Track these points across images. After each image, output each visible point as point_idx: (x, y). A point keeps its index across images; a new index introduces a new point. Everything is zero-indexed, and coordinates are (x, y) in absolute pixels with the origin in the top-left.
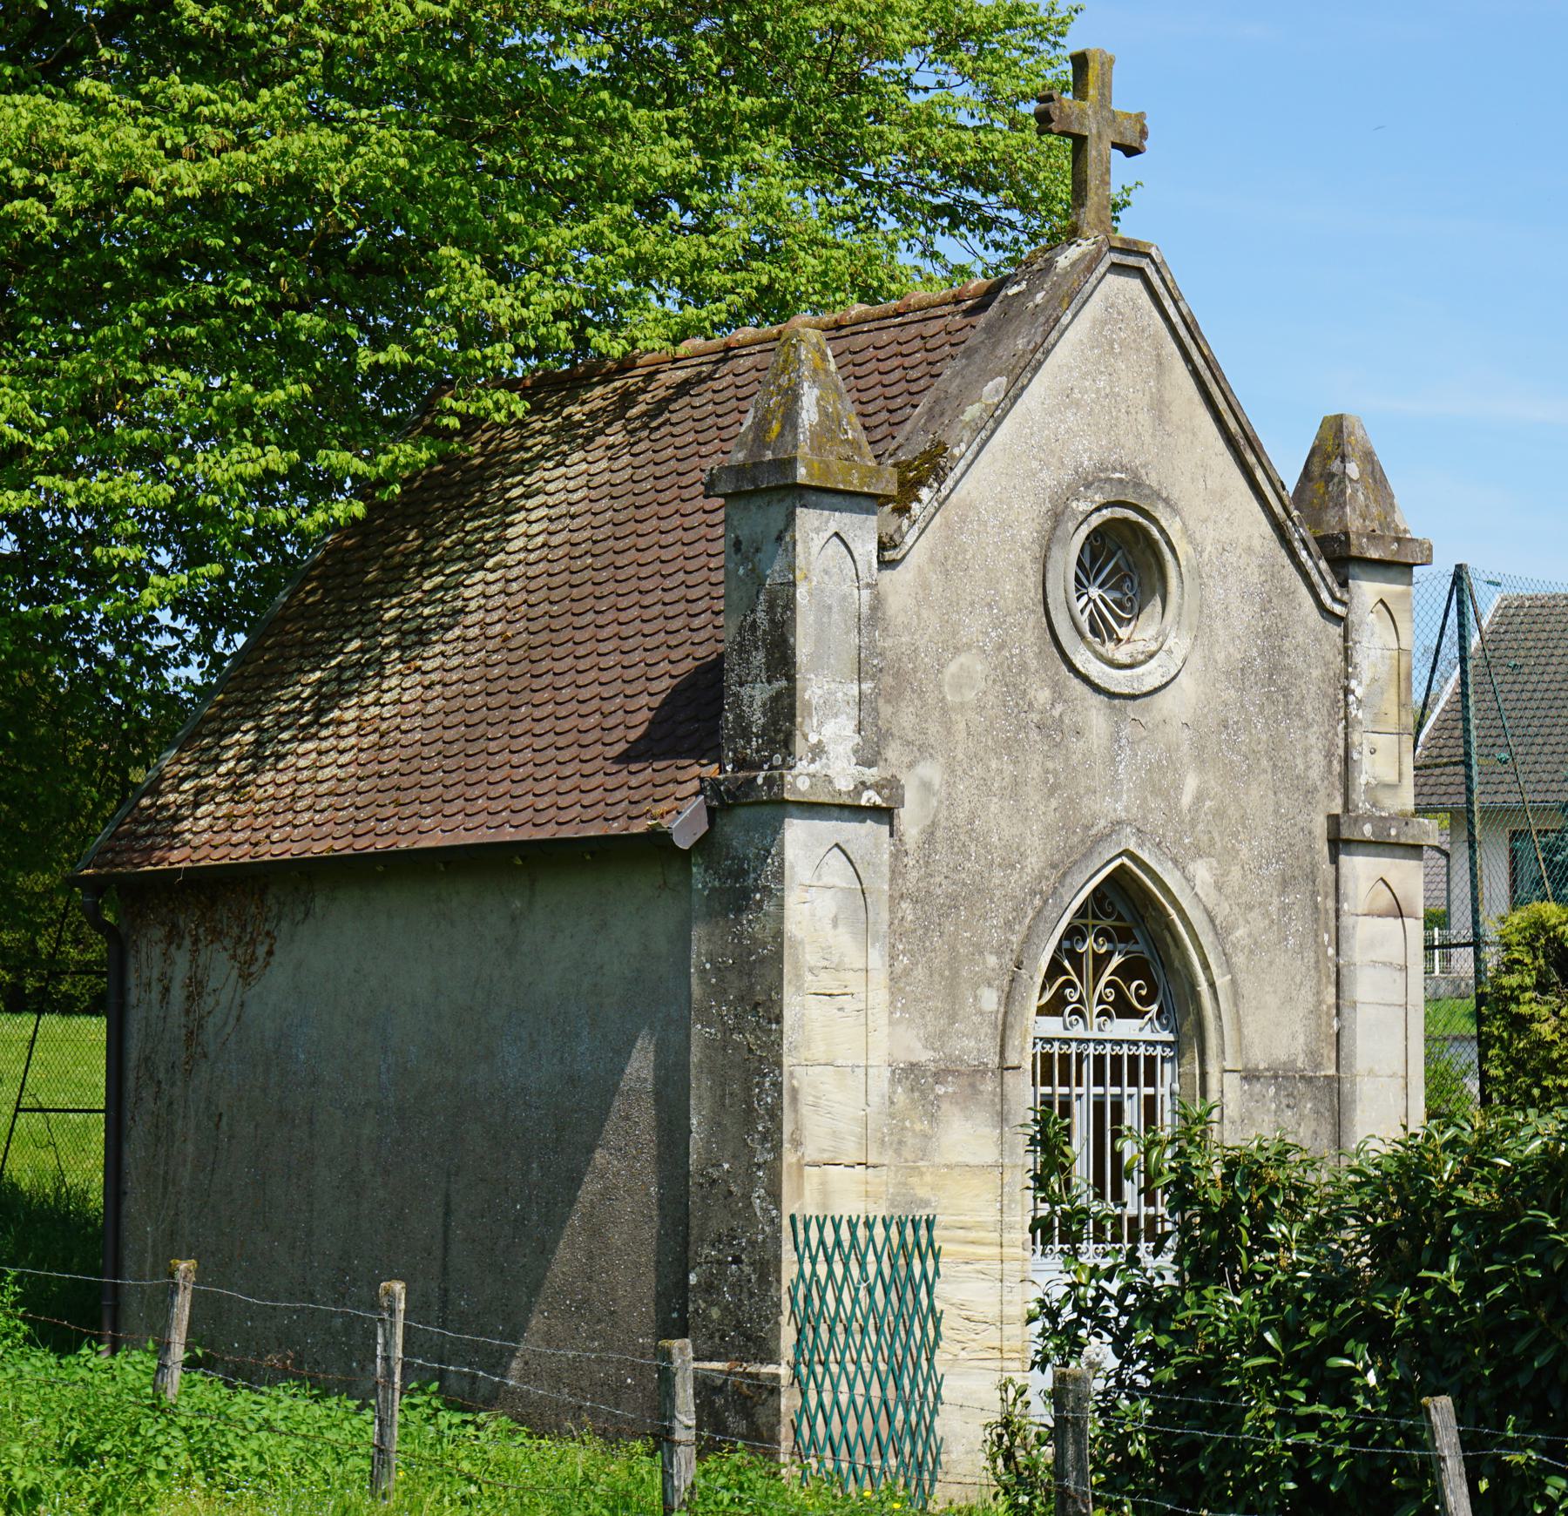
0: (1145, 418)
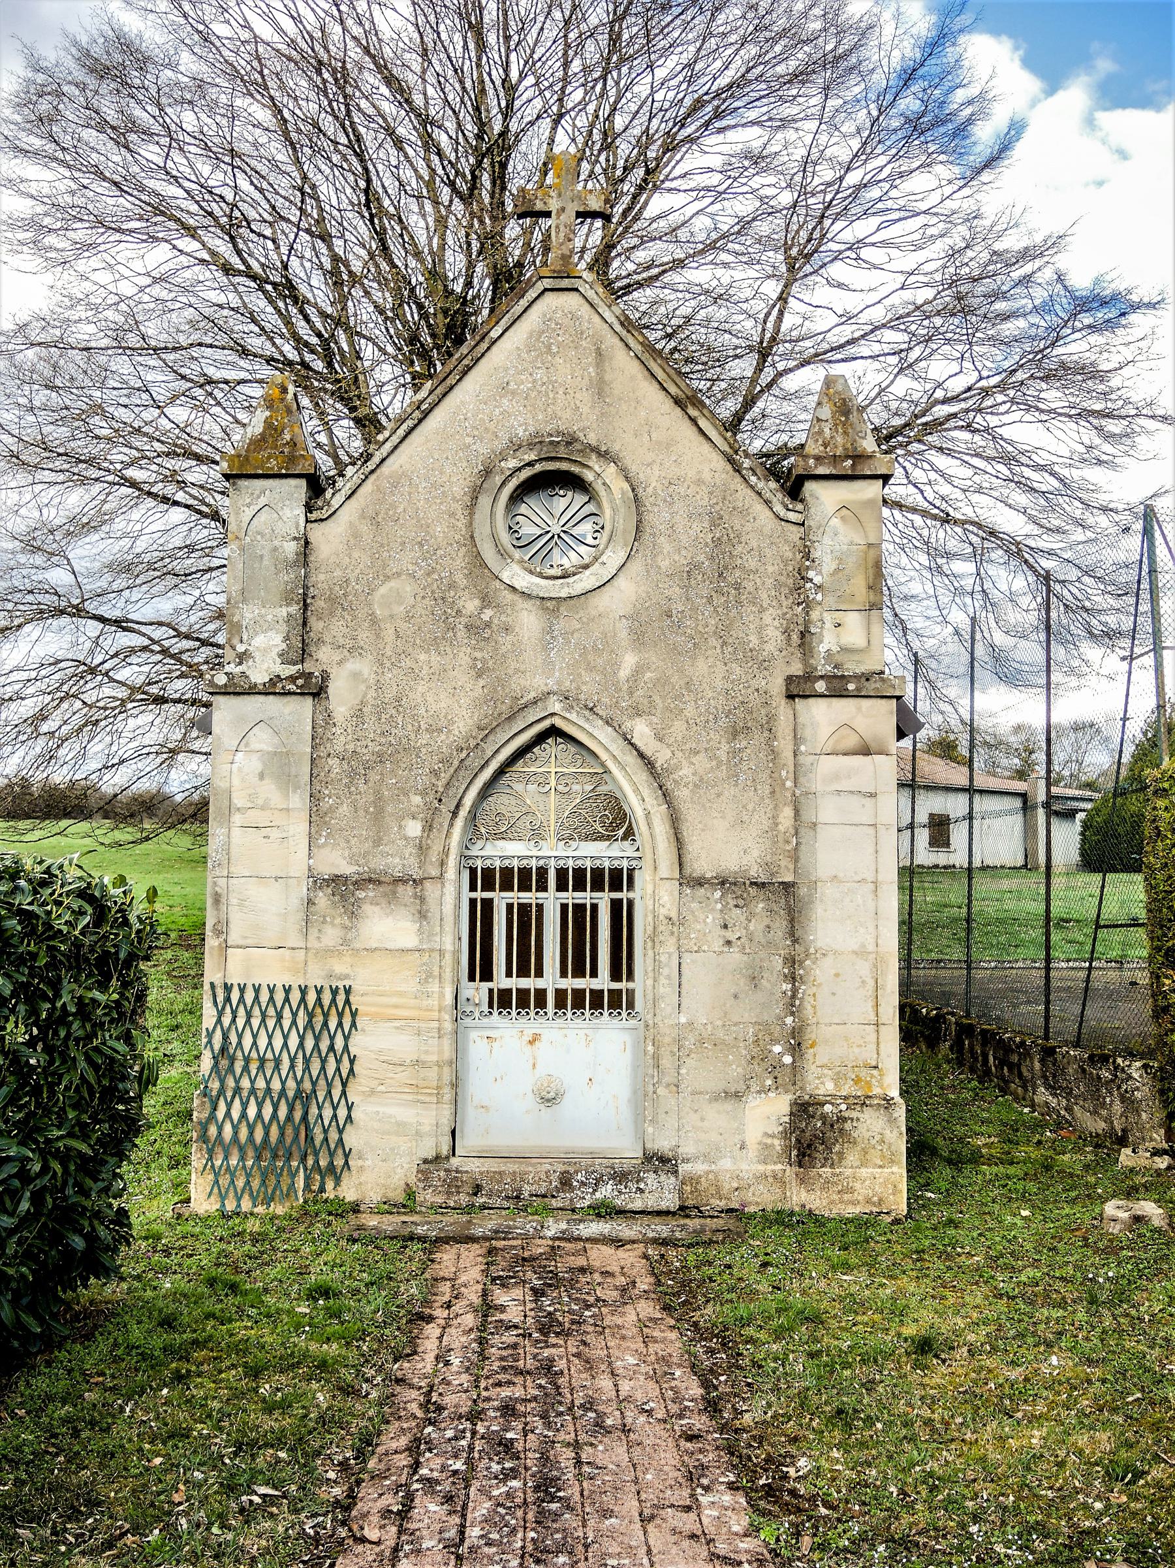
0: (584, 398)
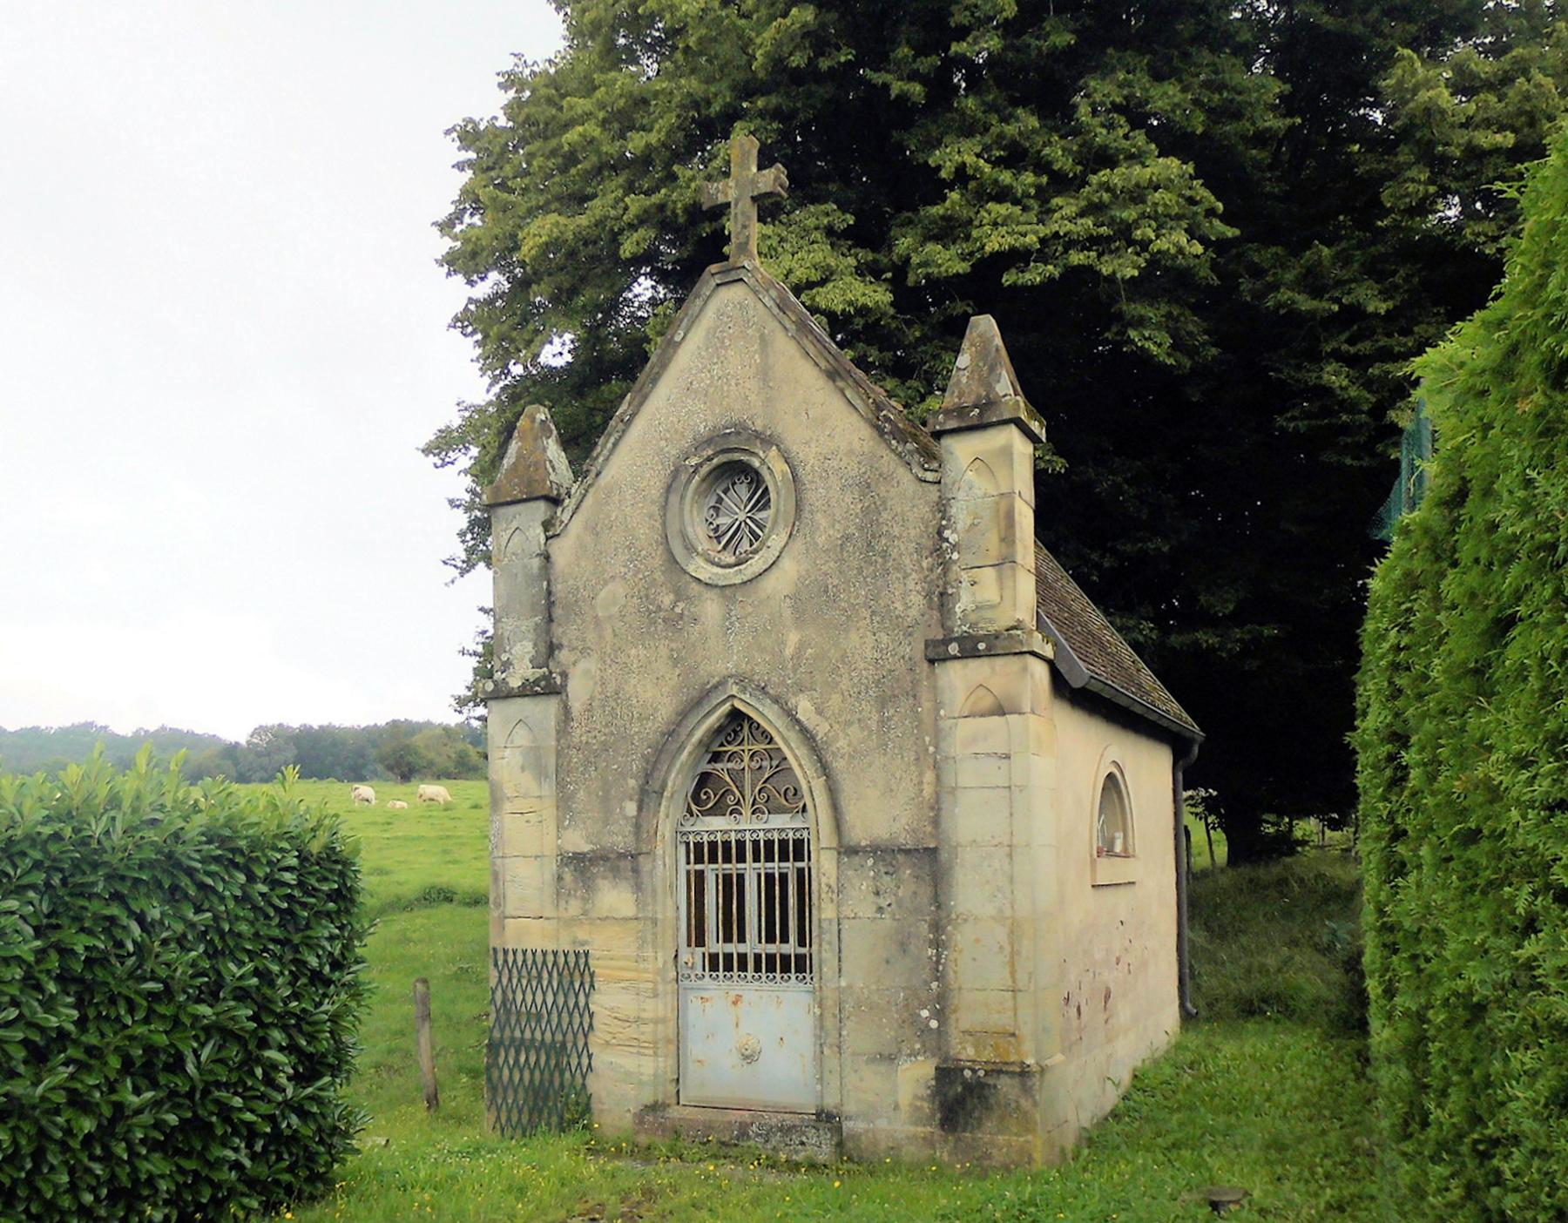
0: (752, 384)
